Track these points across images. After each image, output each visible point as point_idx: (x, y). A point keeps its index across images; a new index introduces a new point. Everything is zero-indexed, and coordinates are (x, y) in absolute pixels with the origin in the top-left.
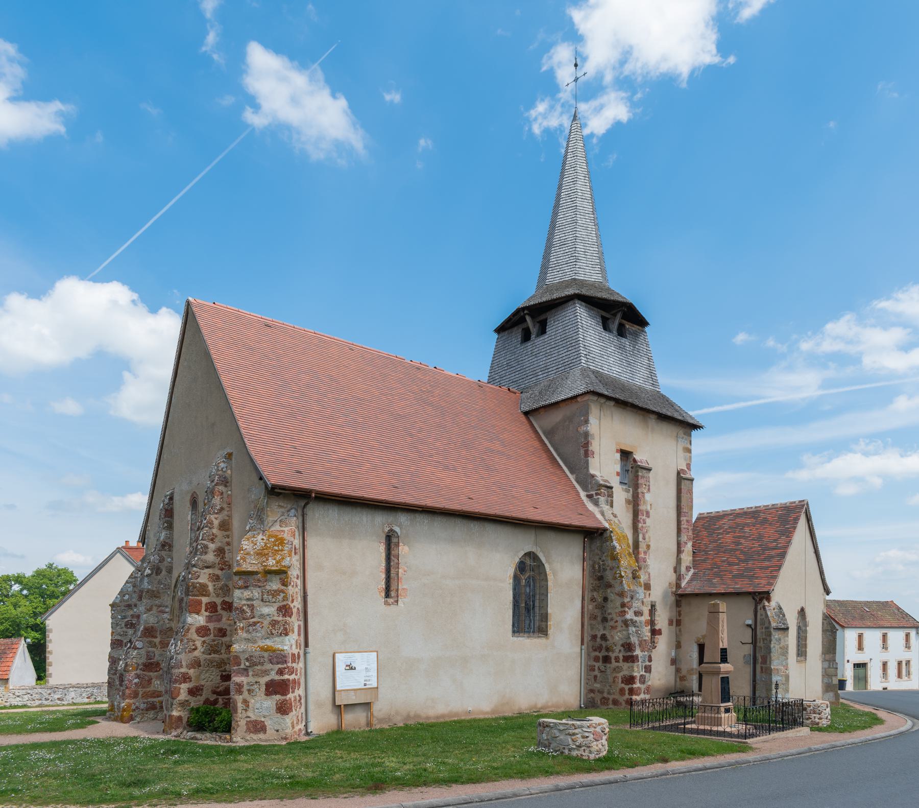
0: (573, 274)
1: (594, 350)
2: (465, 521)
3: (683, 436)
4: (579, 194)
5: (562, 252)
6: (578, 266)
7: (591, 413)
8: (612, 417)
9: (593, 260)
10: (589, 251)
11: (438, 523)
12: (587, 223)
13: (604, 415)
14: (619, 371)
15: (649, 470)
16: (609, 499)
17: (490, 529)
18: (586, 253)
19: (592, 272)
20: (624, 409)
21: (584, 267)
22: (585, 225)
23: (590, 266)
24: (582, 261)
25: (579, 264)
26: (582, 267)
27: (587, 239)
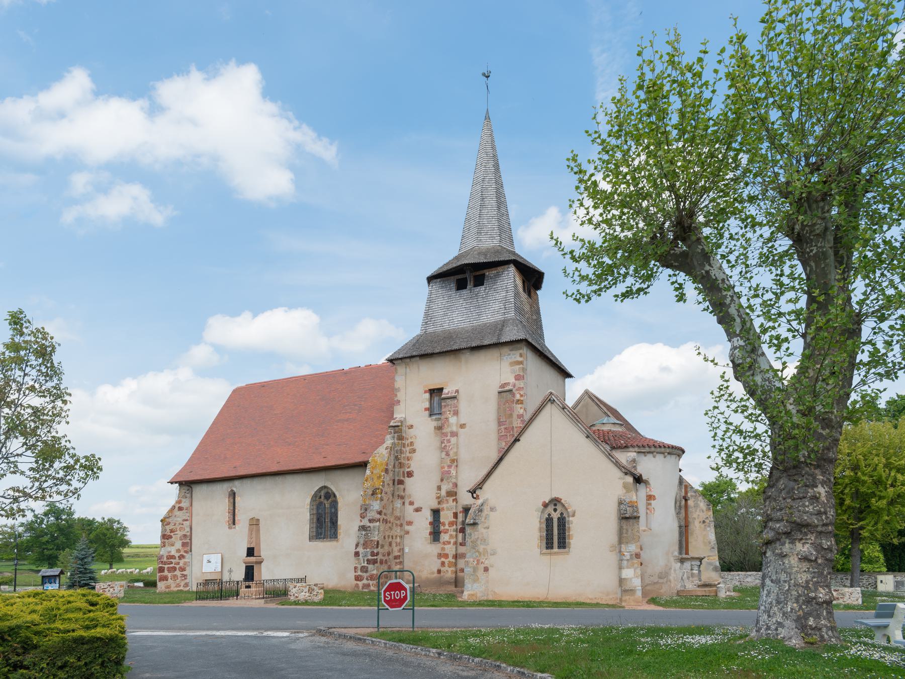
2: (272, 477)
3: (509, 352)
11: (256, 481)
17: (290, 479)
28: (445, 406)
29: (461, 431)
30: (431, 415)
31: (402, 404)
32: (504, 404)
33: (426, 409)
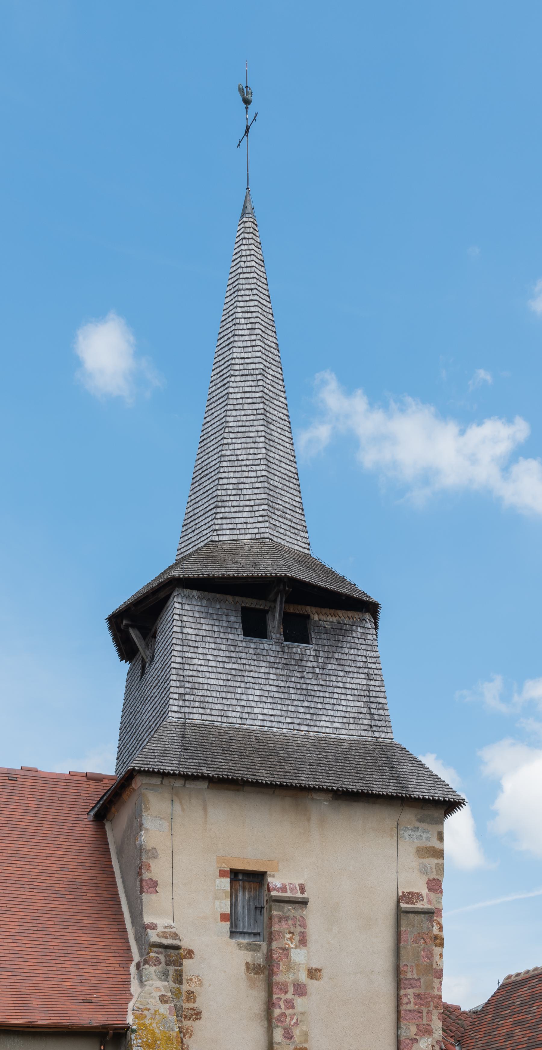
0: (211, 533)
1: (206, 681)
3: (417, 824)
4: (237, 367)
5: (201, 492)
6: (221, 515)
7: (147, 809)
8: (205, 809)
9: (255, 497)
10: (245, 480)
12: (248, 423)
13: (183, 809)
14: (271, 712)
15: (304, 903)
16: (171, 969)
18: (241, 486)
19: (250, 520)
20: (238, 790)
21: (234, 515)
22: (243, 429)
23: (247, 509)
24: (230, 504)
25: (223, 510)
26: (229, 515)
27: (244, 457)
28: (280, 919)
29: (312, 985)
30: (233, 933)
31: (163, 896)
32: (415, 941)
33: (224, 917)
